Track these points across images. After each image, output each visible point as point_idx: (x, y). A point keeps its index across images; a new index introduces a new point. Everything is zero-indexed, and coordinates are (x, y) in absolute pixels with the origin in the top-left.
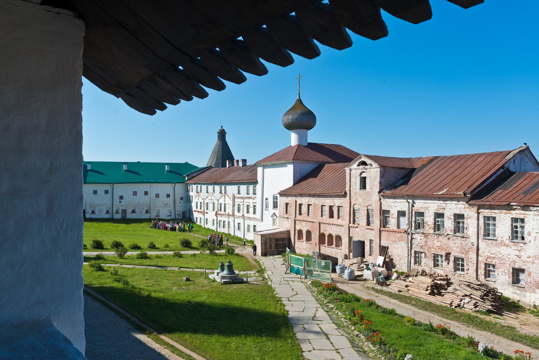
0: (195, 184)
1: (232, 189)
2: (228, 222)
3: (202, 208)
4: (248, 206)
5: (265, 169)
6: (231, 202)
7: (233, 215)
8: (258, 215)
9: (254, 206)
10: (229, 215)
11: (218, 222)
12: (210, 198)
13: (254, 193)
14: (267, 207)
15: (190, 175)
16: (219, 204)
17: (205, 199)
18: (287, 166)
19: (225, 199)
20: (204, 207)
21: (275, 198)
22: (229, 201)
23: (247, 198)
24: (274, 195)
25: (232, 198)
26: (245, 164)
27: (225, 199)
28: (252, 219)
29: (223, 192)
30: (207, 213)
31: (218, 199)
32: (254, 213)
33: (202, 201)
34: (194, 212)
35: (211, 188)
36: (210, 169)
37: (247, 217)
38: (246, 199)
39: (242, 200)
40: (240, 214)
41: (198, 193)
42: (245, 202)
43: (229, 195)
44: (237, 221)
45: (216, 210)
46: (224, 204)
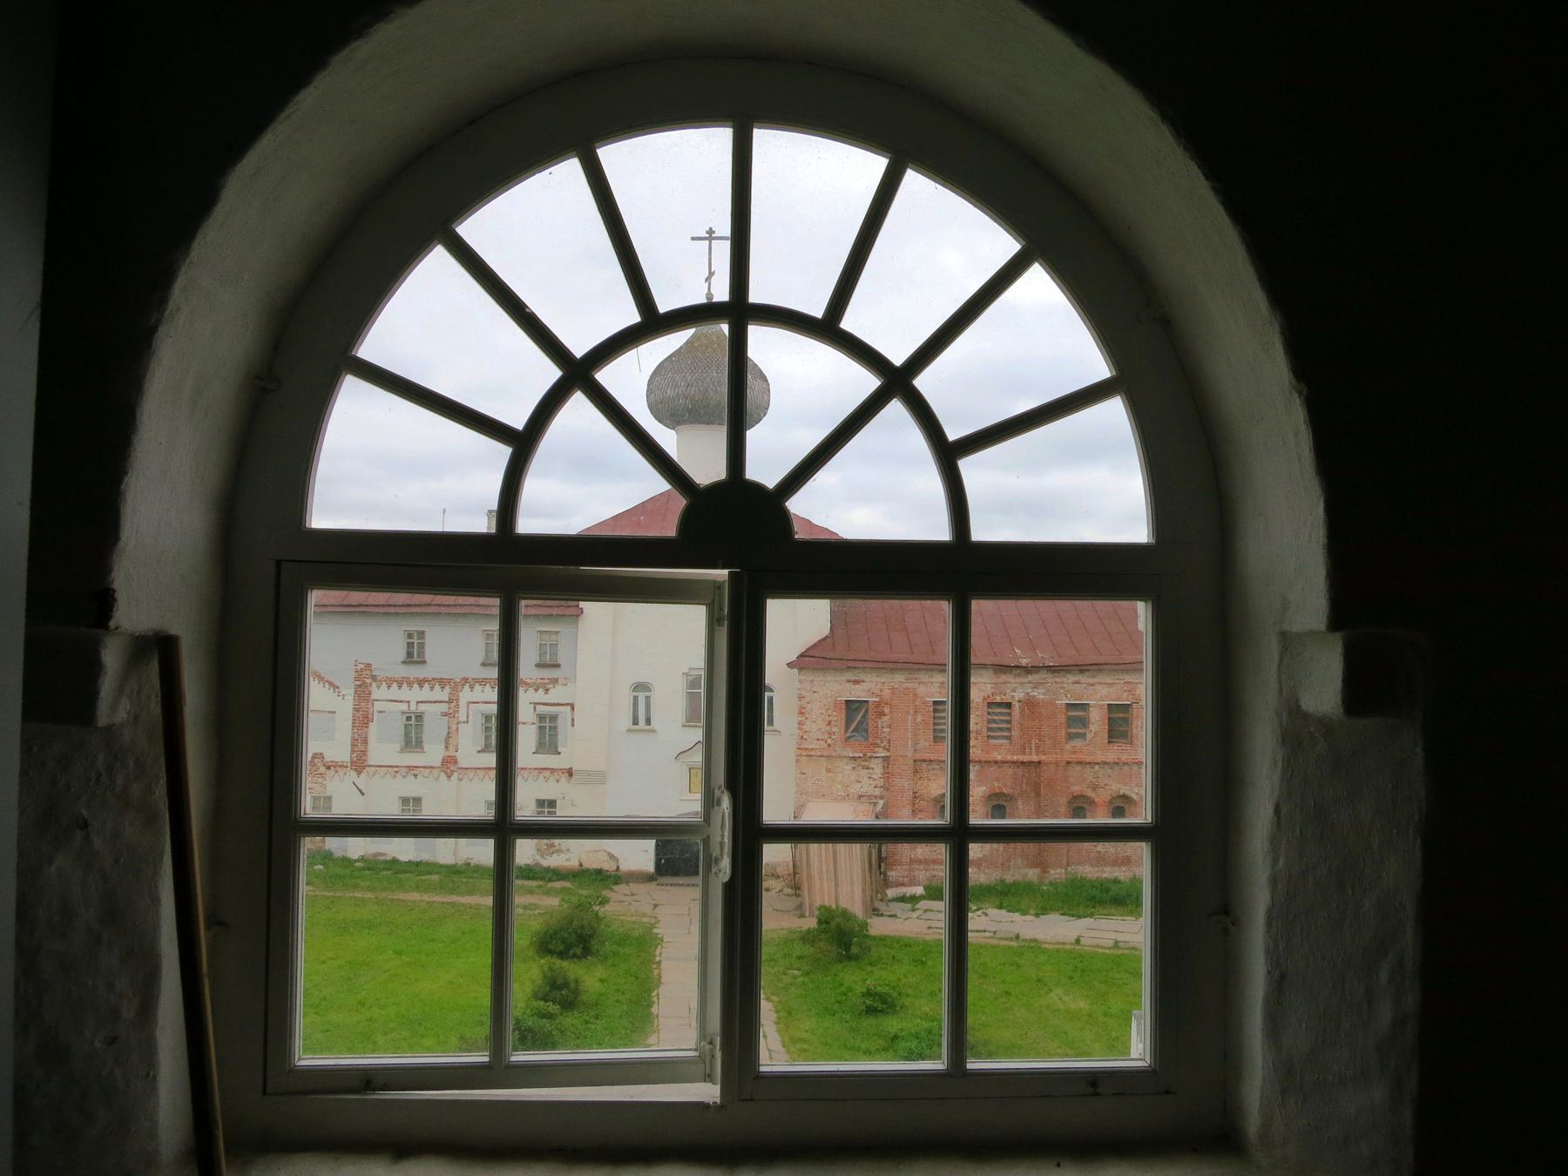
38: (477, 687)
39: (442, 694)
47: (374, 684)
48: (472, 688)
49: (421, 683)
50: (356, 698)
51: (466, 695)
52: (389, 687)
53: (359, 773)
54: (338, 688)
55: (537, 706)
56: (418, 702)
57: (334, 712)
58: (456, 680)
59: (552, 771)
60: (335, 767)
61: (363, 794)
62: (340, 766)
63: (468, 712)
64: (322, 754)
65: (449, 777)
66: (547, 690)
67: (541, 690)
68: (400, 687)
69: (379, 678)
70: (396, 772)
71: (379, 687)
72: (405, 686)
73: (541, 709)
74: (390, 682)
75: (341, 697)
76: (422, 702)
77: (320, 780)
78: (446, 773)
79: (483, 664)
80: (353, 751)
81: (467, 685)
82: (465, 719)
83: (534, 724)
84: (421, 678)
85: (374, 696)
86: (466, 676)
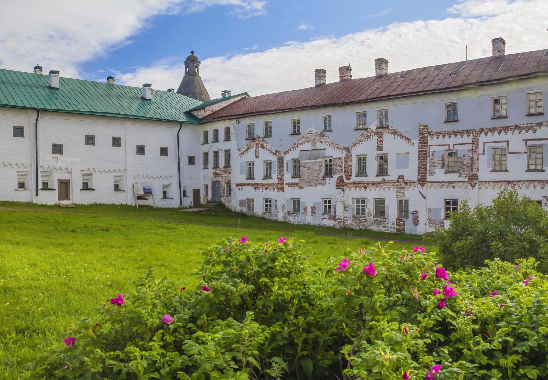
2: (400, 202)
6: (414, 150)
15: (207, 108)
20: (281, 171)
33: (274, 159)
38: (490, 133)
39: (470, 139)
41: (254, 139)
43: (401, 130)
47: (429, 137)
48: (486, 134)
49: (455, 134)
50: (420, 145)
51: (482, 138)
52: (438, 138)
53: (422, 186)
54: (410, 140)
55: (530, 143)
56: (454, 145)
57: (409, 153)
58: (477, 130)
59: (539, 182)
60: (409, 183)
61: (425, 198)
62: (413, 182)
63: (484, 148)
64: (403, 176)
65: (473, 187)
66: (535, 131)
67: (531, 131)
68: (444, 137)
69: (432, 133)
70: (443, 185)
71: (432, 138)
72: (447, 136)
73: (530, 143)
74: (438, 134)
75: (412, 145)
76: (456, 144)
77: (402, 190)
78: (471, 185)
79: (493, 118)
80: (419, 174)
81: (483, 133)
82: (482, 152)
83: (526, 153)
84: (456, 130)
85: (429, 144)
86: (483, 127)
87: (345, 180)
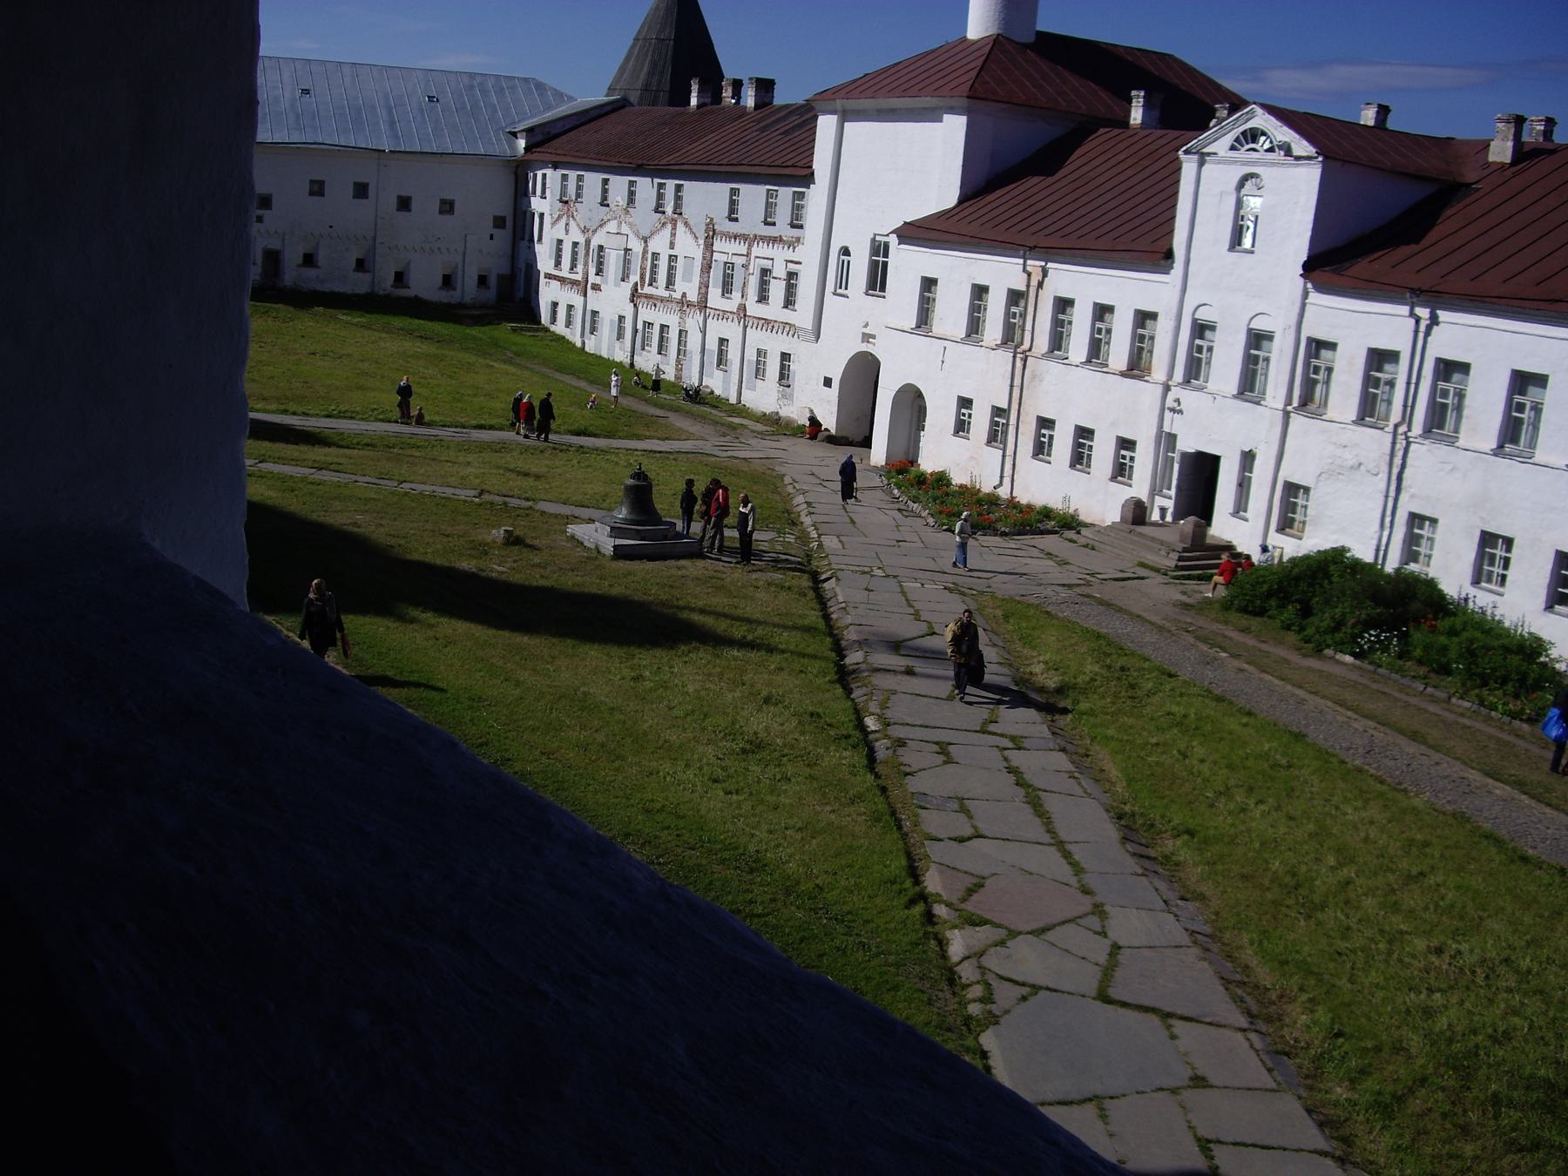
0: (555, 166)
1: (706, 197)
3: (580, 268)
4: (765, 272)
5: (846, 124)
6: (698, 253)
7: (703, 305)
8: (802, 315)
9: (792, 276)
10: (684, 303)
11: (640, 326)
12: (612, 226)
13: (796, 225)
14: (843, 281)
16: (650, 256)
17: (595, 231)
18: (941, 121)
19: (673, 235)
20: (586, 264)
21: (879, 249)
22: (689, 247)
23: (763, 239)
24: (875, 235)
25: (702, 235)
26: (767, 100)
27: (673, 235)
28: (776, 325)
29: (669, 209)
30: (596, 287)
31: (647, 234)
32: (789, 302)
33: (581, 239)
34: (542, 280)
35: (619, 184)
36: (623, 107)
37: (759, 318)
39: (743, 249)
40: (731, 305)
41: (566, 202)
42: (752, 257)
43: (691, 222)
44: (716, 329)
45: (635, 278)
46: (670, 256)
87: (640, 291)
